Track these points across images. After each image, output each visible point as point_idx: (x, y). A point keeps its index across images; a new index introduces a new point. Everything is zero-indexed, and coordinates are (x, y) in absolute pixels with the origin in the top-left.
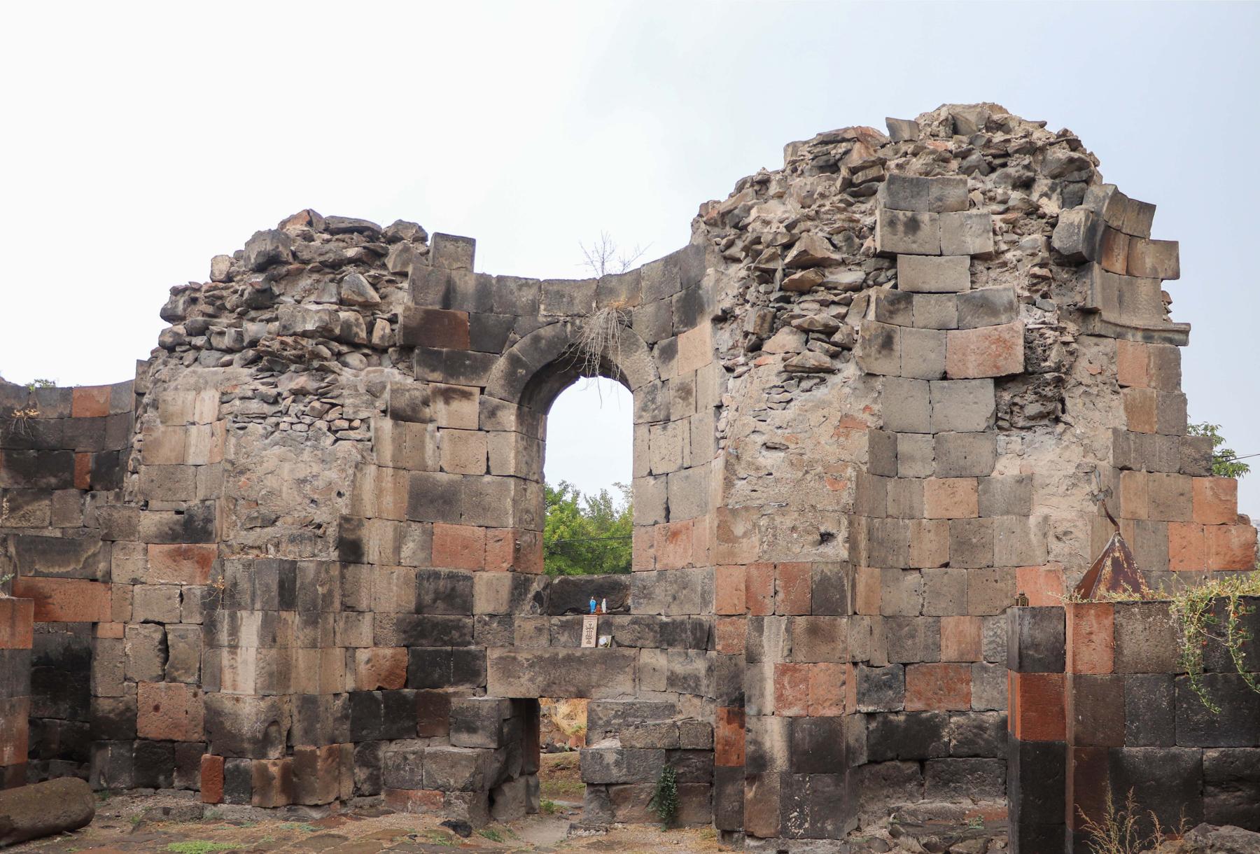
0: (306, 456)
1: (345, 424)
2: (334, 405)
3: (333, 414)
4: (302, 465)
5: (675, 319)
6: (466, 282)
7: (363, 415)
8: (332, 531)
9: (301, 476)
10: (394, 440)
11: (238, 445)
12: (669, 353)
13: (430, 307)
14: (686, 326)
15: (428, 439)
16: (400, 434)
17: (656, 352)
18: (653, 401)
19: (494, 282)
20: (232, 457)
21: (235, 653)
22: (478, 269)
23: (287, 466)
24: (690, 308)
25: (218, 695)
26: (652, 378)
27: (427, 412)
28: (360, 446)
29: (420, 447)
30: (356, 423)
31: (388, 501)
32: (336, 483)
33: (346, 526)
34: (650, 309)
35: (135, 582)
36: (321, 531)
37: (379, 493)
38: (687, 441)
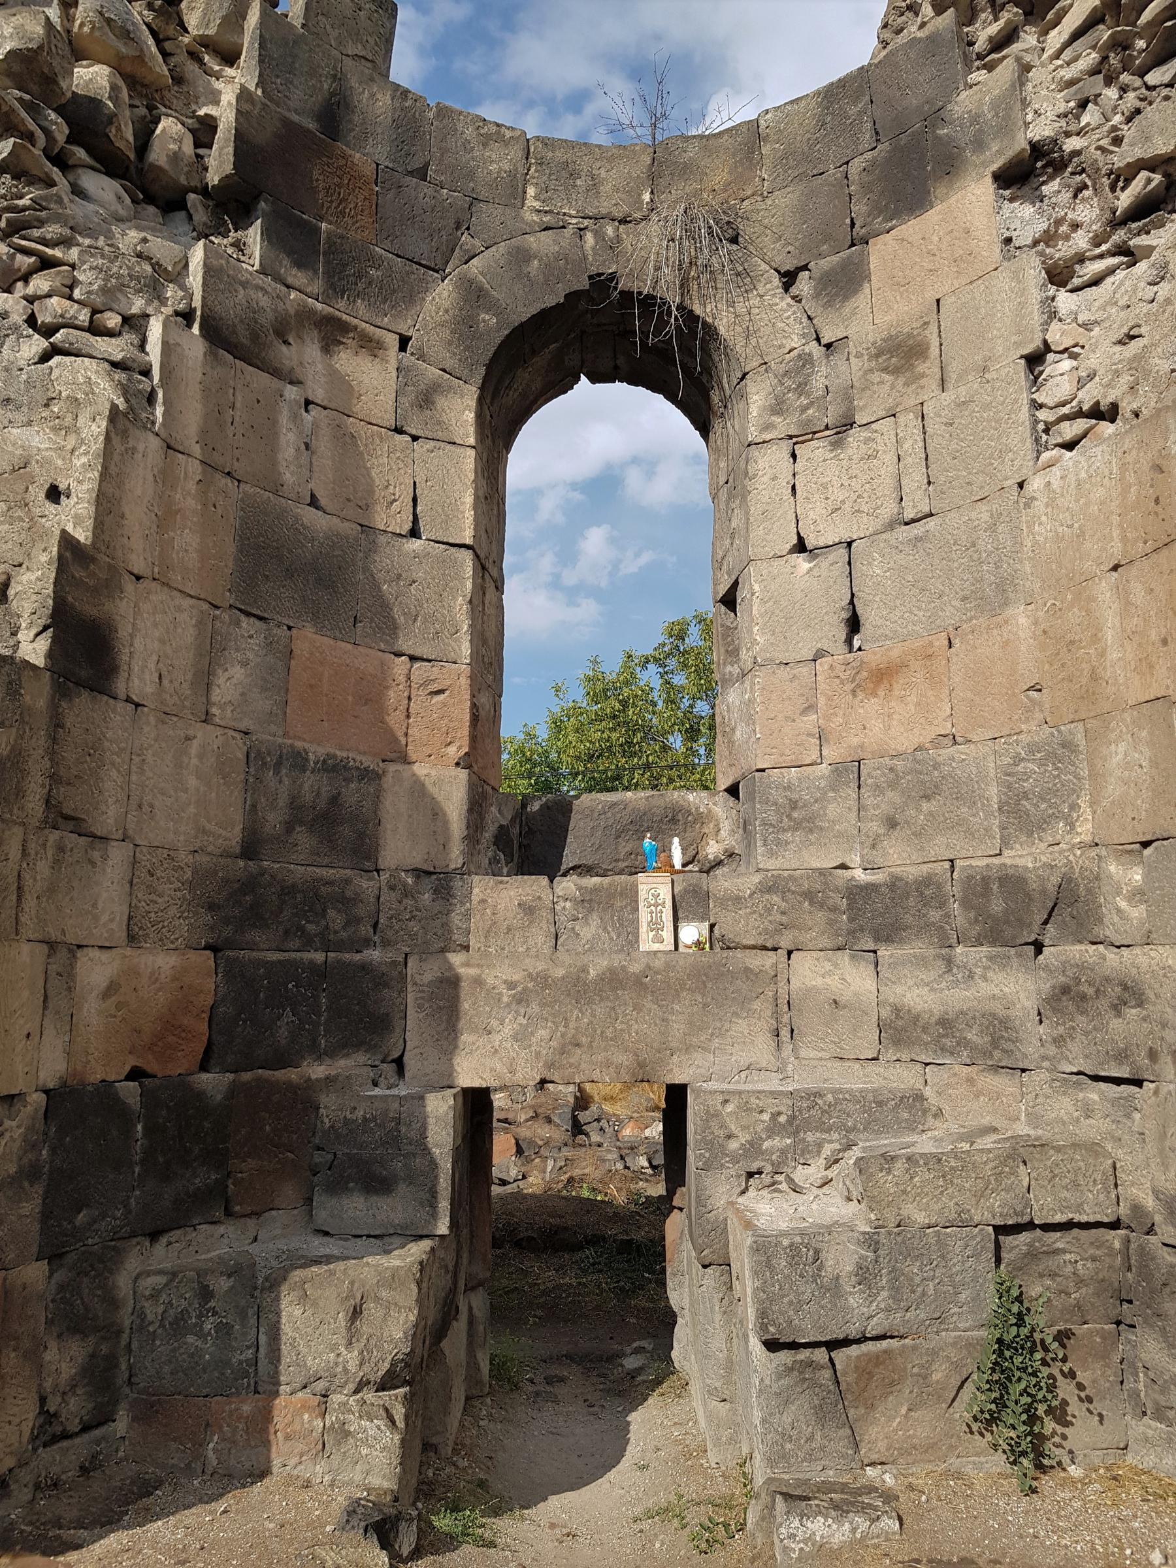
2: (46, 264)
5: (859, 208)
12: (845, 282)
13: (295, 118)
14: (886, 220)
15: (284, 419)
17: (804, 284)
18: (801, 389)
19: (431, 115)
24: (912, 169)
26: (796, 342)
27: (287, 355)
29: (268, 434)
30: (112, 321)
31: (187, 541)
32: (44, 463)
33: (79, 573)
34: (785, 200)
38: (913, 460)
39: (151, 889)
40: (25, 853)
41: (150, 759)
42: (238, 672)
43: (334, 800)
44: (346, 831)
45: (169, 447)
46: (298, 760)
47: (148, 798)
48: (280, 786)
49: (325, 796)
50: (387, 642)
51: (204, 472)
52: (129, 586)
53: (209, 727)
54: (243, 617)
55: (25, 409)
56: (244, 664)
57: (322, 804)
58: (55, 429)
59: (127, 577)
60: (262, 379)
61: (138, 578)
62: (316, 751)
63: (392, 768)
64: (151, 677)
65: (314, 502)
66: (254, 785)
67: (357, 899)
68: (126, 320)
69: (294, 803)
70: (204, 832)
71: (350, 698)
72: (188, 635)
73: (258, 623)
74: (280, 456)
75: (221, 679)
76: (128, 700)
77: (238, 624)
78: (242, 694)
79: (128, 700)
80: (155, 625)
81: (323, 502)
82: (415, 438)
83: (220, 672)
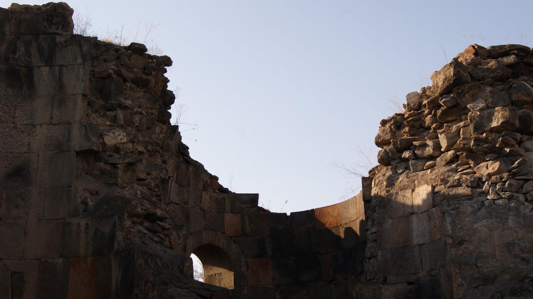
0: (511, 222)
2: (526, 181)
11: (453, 223)
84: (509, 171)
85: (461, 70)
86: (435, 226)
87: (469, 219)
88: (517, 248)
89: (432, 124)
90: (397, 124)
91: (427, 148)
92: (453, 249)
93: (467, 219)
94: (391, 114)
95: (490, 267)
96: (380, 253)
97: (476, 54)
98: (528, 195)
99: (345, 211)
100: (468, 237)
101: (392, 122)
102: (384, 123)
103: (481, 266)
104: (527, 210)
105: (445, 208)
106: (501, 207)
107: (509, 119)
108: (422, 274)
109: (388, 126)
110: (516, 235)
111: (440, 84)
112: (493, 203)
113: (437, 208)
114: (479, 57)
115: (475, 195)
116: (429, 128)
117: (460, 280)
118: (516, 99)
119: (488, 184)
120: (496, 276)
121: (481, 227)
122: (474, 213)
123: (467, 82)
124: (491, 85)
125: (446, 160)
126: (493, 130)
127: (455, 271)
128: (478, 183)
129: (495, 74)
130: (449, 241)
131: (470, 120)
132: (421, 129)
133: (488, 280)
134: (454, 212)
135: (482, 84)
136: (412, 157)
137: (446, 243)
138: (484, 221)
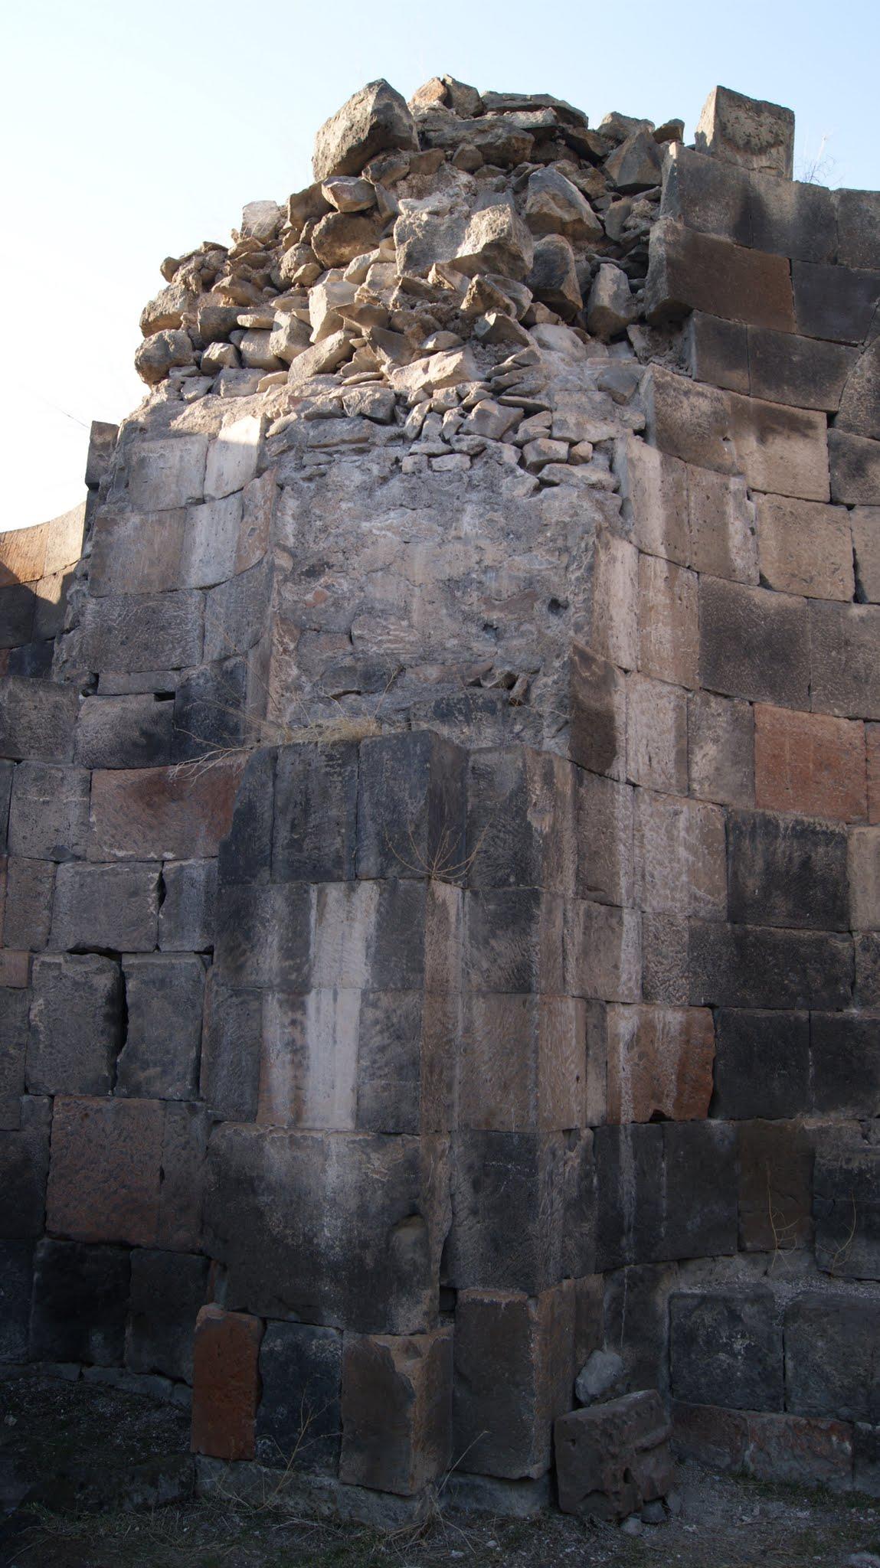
0: (468, 523)
1: (562, 449)
2: (530, 412)
3: (532, 426)
4: (459, 546)
6: (779, 198)
7: (598, 431)
8: (545, 684)
9: (457, 570)
10: (666, 499)
13: (714, 236)
15: (730, 509)
16: (678, 487)
20: (291, 542)
21: (302, 1007)
22: (800, 172)
23: (420, 552)
25: (250, 1132)
28: (598, 495)
30: (584, 449)
31: (662, 632)
35: (58, 856)
36: (518, 688)
37: (643, 615)
39: (658, 953)
40: (566, 921)
41: (648, 834)
42: (711, 749)
43: (806, 863)
44: (818, 893)
45: (641, 551)
46: (769, 827)
47: (649, 868)
48: (756, 854)
49: (797, 861)
50: (840, 708)
51: (670, 570)
52: (621, 680)
53: (693, 802)
54: (712, 698)
55: (524, 538)
56: (716, 741)
57: (795, 869)
58: (550, 551)
59: (618, 672)
60: (711, 478)
61: (626, 671)
62: (787, 818)
63: (857, 830)
64: (643, 759)
65: (763, 583)
66: (733, 855)
67: (834, 957)
68: (595, 445)
69: (769, 868)
70: (696, 899)
71: (811, 766)
72: (670, 719)
73: (725, 702)
74: (730, 544)
75: (698, 756)
76: (628, 782)
77: (707, 703)
78: (717, 769)
79: (628, 782)
80: (643, 713)
81: (771, 580)
82: (850, 507)
83: (696, 750)
84: (488, 380)
85: (395, 104)
86: (253, 530)
87: (350, 505)
88: (475, 594)
89: (298, 265)
90: (204, 271)
91: (273, 335)
92: (289, 584)
93: (344, 506)
94: (198, 245)
95: (390, 641)
96: (92, 605)
97: (447, 99)
98: (527, 448)
99: (58, 541)
100: (340, 555)
101: (192, 265)
102: (170, 268)
103: (360, 637)
104: (520, 491)
105: (288, 472)
106: (446, 477)
107: (509, 234)
108: (200, 671)
109: (178, 277)
110: (476, 557)
111: (333, 150)
112: (425, 464)
113: (266, 475)
114: (453, 111)
115: (377, 441)
116: (288, 284)
117: (295, 671)
118: (535, 210)
119: (420, 411)
120: (402, 670)
121: (381, 529)
122: (368, 489)
123: (406, 144)
124: (471, 172)
125: (317, 362)
126: (457, 266)
127: (282, 643)
128: (393, 411)
129: (489, 139)
130: (284, 561)
131: (398, 235)
132: (267, 289)
133: (372, 678)
134: (313, 486)
135: (449, 159)
136: (231, 358)
137: (273, 568)
138: (392, 514)
